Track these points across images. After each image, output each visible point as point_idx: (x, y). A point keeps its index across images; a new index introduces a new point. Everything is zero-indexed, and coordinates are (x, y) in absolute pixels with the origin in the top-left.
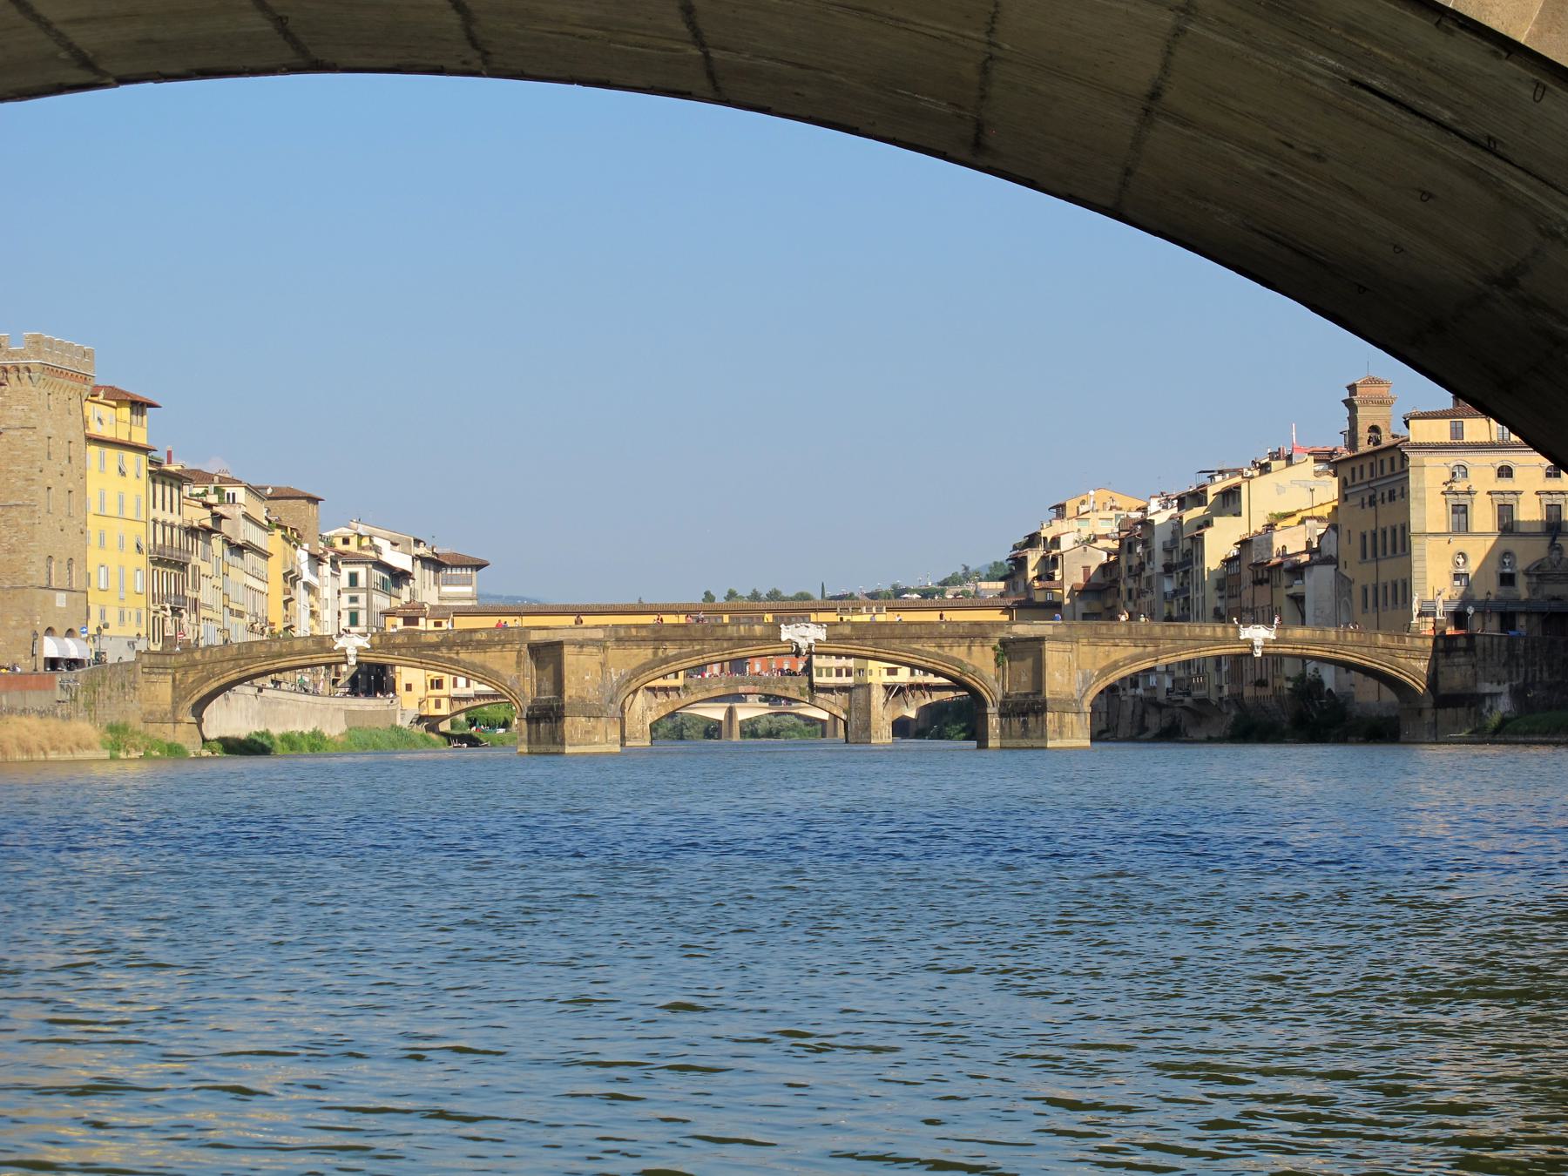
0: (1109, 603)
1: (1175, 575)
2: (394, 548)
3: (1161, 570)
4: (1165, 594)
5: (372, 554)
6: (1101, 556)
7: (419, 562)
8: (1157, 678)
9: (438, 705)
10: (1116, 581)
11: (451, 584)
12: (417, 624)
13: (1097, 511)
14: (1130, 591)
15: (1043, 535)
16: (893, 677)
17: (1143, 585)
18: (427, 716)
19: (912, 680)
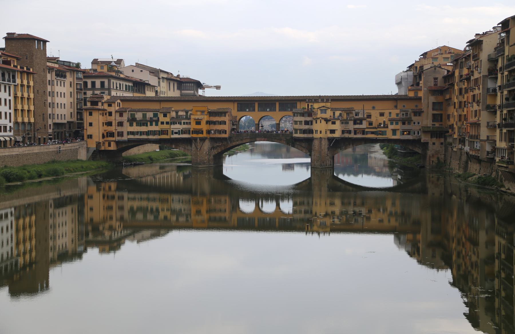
0: (448, 97)
1: (499, 76)
2: (151, 74)
3: (487, 74)
4: (488, 89)
5: (114, 74)
6: (444, 72)
7: (165, 81)
8: (481, 145)
9: (109, 145)
10: (453, 85)
11: (186, 90)
12: (97, 105)
13: (442, 54)
14: (460, 90)
15: (415, 66)
16: (333, 134)
17: (472, 84)
18: (105, 151)
19: (343, 136)
